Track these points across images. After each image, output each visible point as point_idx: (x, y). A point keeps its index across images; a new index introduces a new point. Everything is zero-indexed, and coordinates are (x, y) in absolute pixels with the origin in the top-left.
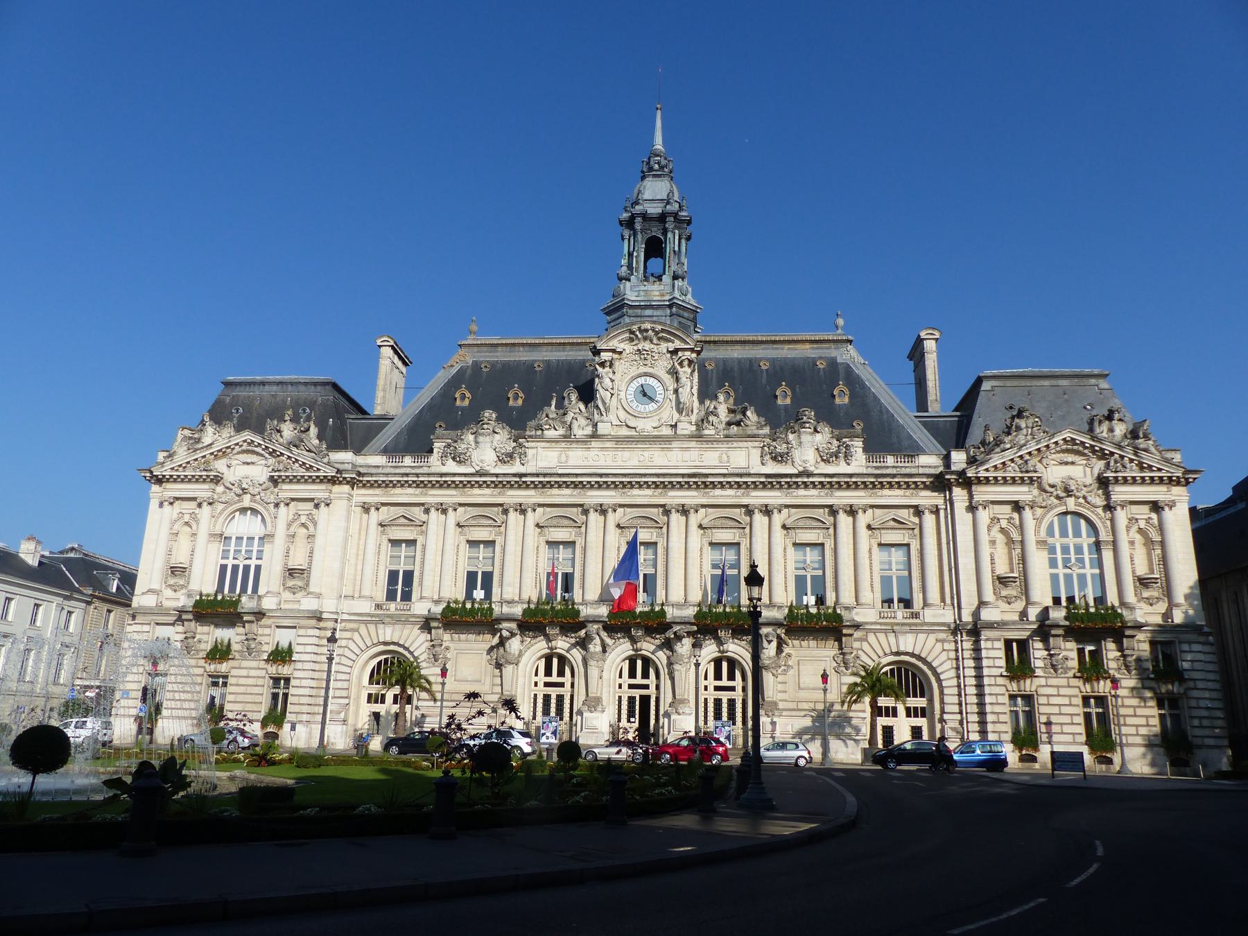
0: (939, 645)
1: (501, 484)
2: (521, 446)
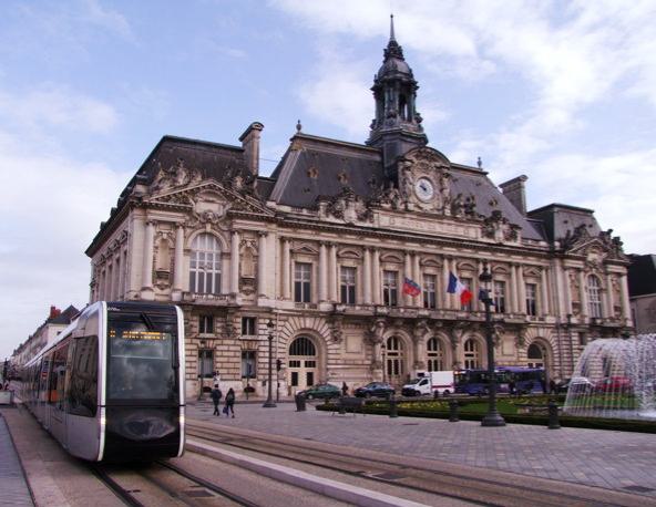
1: (364, 233)
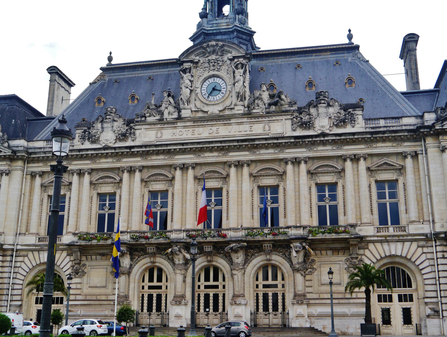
0: (420, 250)
1: (118, 154)
2: (131, 128)
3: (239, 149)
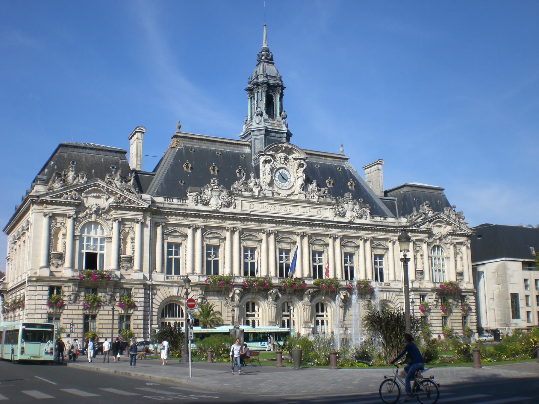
3: (303, 224)
